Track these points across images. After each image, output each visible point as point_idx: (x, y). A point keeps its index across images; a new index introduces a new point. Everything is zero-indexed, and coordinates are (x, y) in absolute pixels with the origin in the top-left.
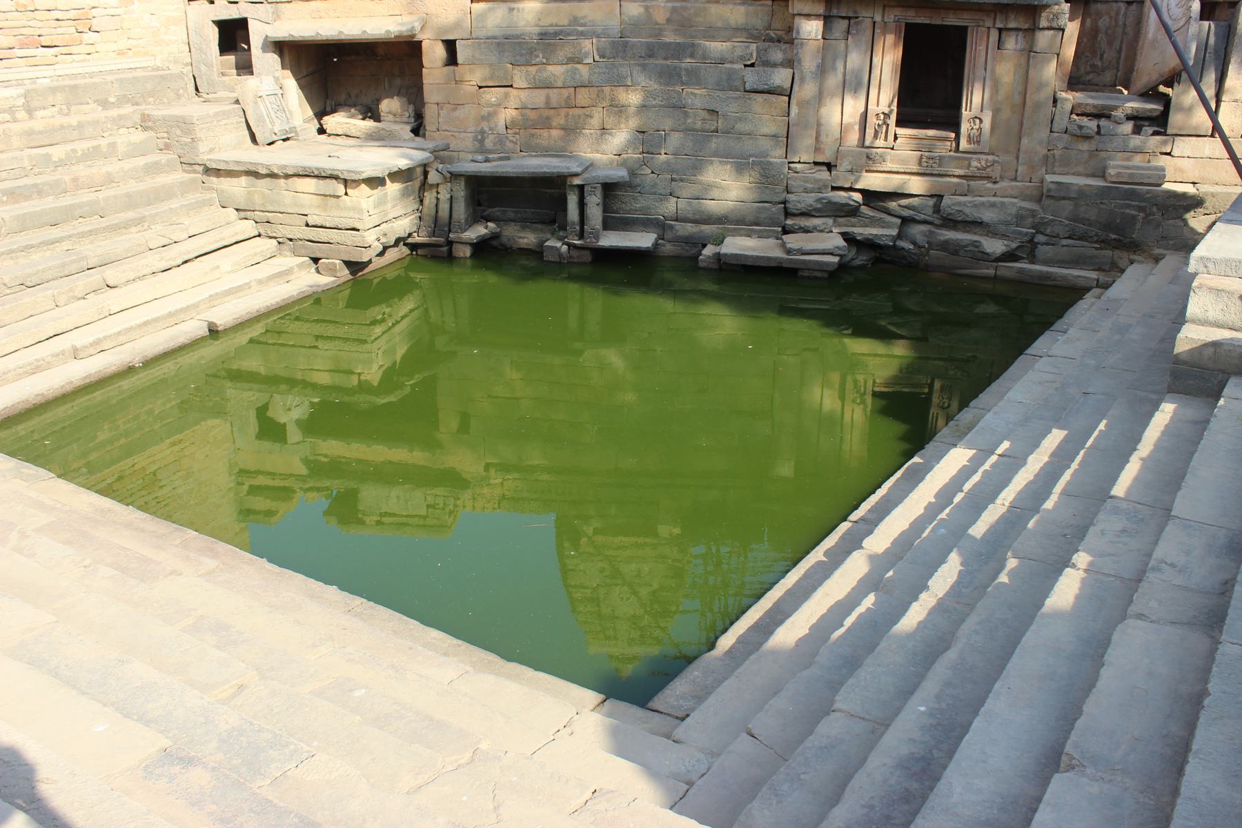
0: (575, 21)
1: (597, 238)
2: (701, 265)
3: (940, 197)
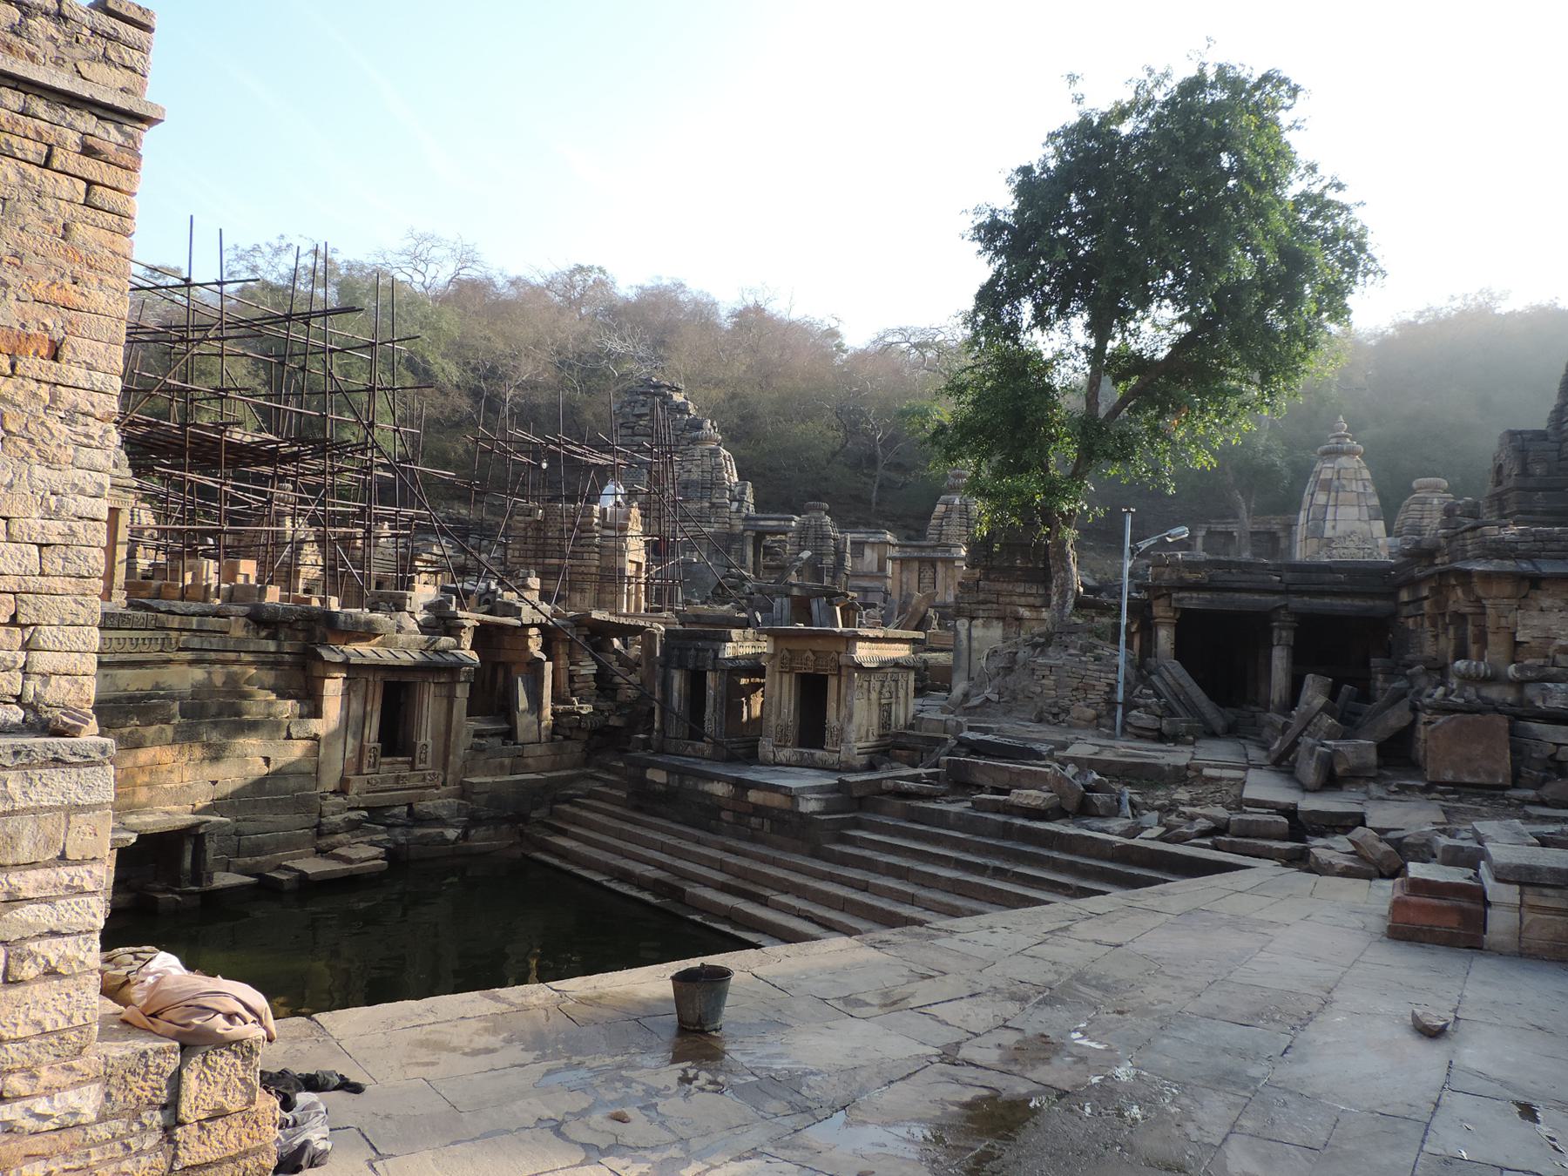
0: (157, 686)
1: (210, 879)
2: (287, 887)
3: (410, 805)
